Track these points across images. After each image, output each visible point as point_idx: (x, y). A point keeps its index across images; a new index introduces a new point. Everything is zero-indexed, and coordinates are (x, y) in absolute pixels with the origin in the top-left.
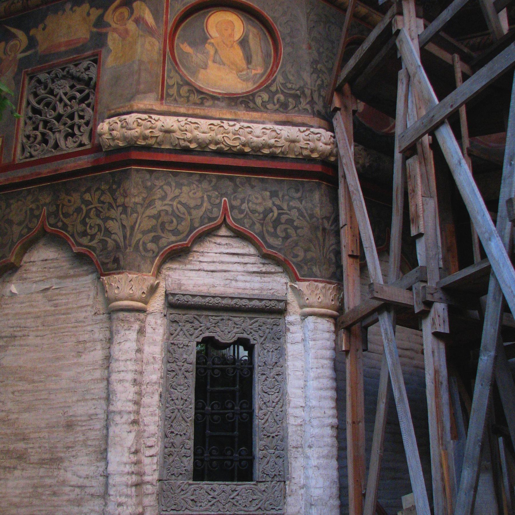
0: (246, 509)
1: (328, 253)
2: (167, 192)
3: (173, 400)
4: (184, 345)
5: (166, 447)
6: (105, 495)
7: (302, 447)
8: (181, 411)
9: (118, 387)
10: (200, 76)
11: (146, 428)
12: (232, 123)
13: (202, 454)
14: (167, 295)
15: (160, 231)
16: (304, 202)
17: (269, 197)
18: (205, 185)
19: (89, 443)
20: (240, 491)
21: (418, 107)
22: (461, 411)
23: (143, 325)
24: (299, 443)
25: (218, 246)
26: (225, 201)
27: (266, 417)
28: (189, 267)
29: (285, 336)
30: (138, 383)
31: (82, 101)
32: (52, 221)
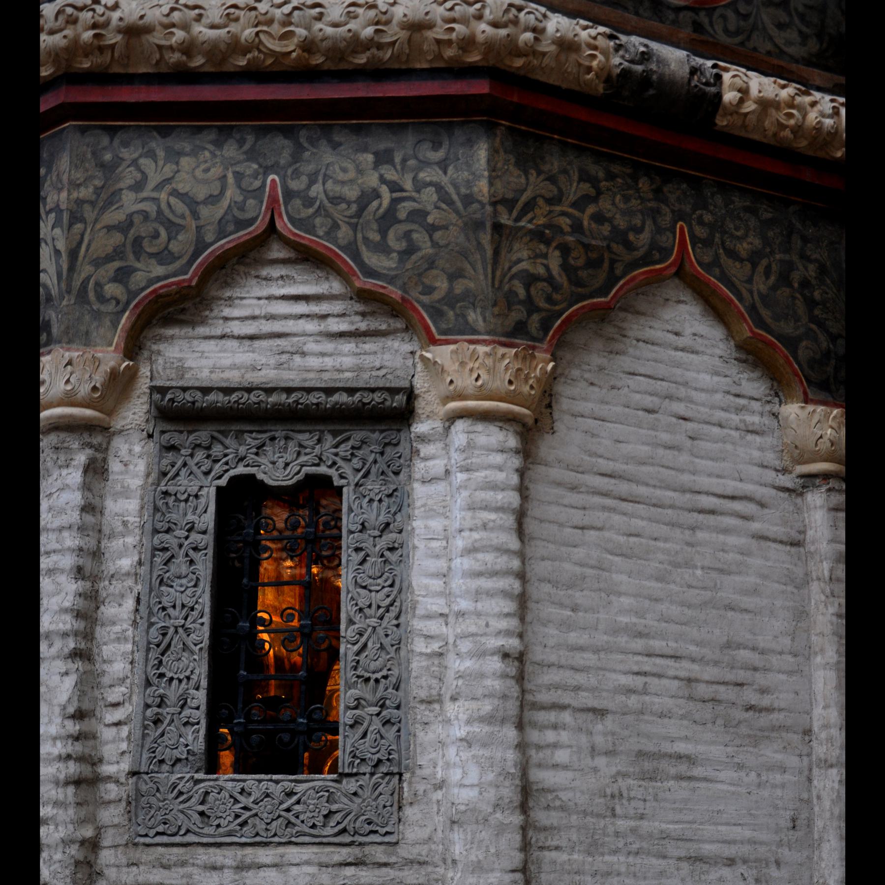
0: (312, 831)
1: (507, 279)
2: (147, 171)
4: (189, 495)
5: (147, 706)
8: (180, 630)
11: (105, 667)
15: (131, 257)
17: (371, 166)
18: (230, 150)
20: (304, 795)
23: (99, 456)
24: (434, 692)
25: (264, 282)
26: (273, 181)
27: (363, 640)
28: (202, 330)
29: (409, 466)
30: (87, 574)
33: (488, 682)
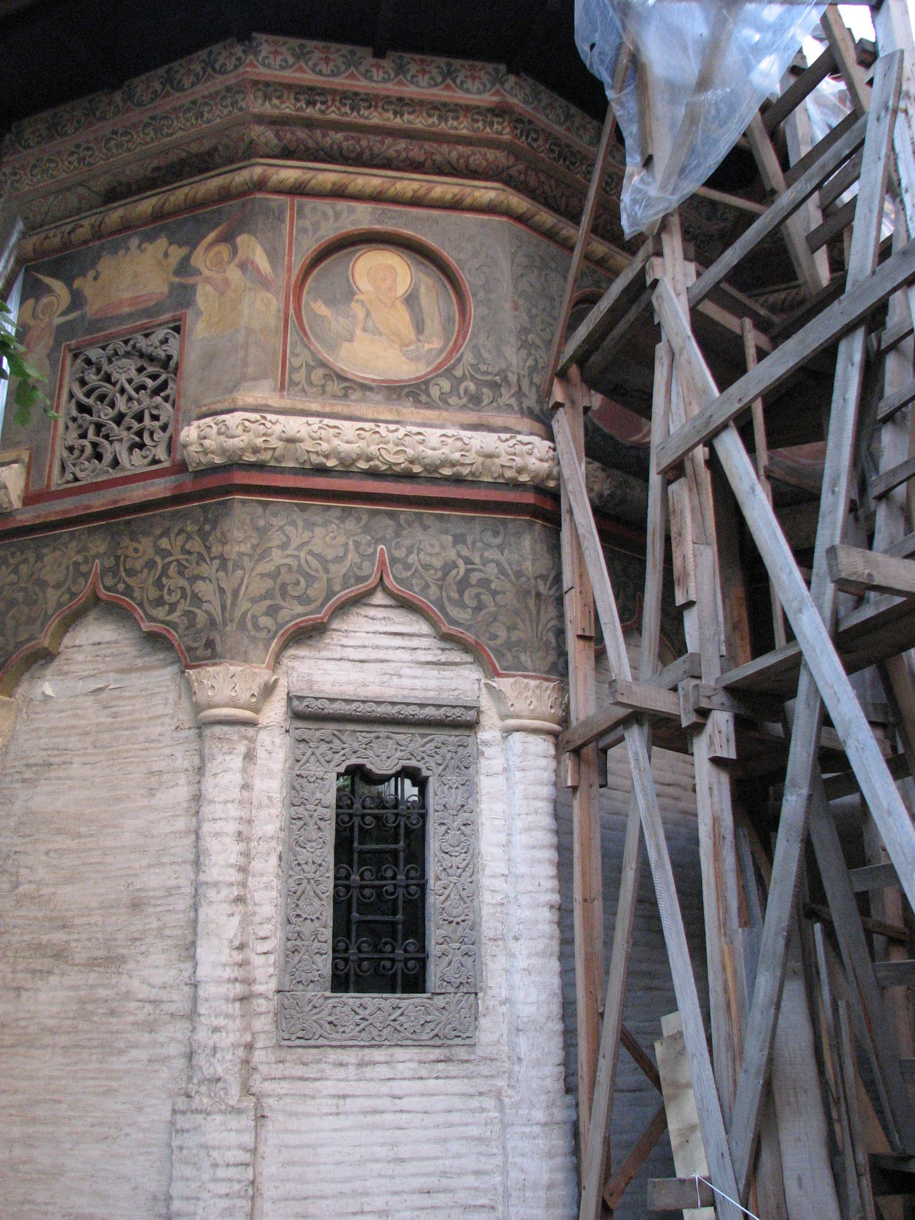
0: (414, 1037)
3: (299, 864)
5: (289, 940)
6: (192, 1015)
7: (503, 939)
9: (212, 844)
10: (343, 353)
11: (257, 909)
12: (392, 427)
13: (346, 950)
14: (290, 699)
15: (279, 597)
16: (506, 552)
18: (350, 524)
19: (167, 932)
21: (687, 401)
22: (754, 883)
24: (499, 933)
27: (447, 892)
28: (325, 654)
31: (156, 392)
32: (109, 581)
33: (541, 927)
